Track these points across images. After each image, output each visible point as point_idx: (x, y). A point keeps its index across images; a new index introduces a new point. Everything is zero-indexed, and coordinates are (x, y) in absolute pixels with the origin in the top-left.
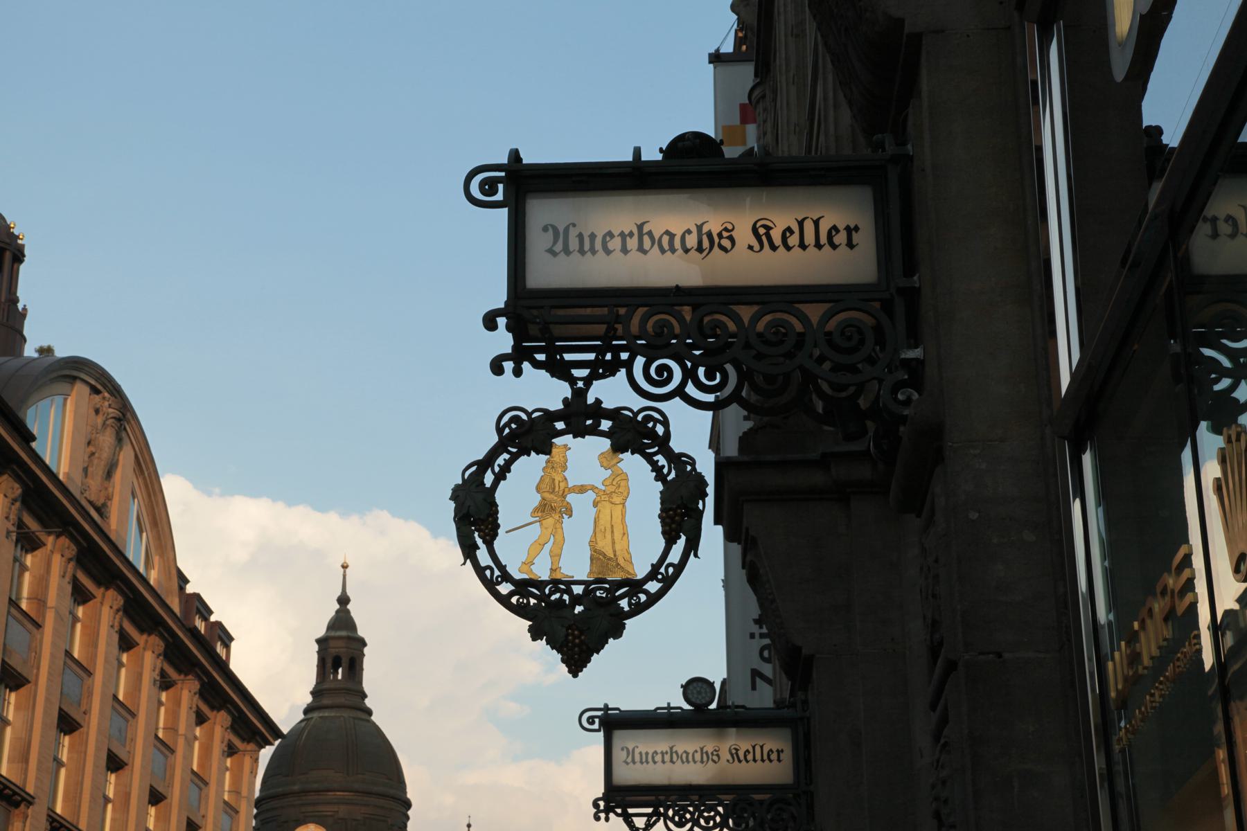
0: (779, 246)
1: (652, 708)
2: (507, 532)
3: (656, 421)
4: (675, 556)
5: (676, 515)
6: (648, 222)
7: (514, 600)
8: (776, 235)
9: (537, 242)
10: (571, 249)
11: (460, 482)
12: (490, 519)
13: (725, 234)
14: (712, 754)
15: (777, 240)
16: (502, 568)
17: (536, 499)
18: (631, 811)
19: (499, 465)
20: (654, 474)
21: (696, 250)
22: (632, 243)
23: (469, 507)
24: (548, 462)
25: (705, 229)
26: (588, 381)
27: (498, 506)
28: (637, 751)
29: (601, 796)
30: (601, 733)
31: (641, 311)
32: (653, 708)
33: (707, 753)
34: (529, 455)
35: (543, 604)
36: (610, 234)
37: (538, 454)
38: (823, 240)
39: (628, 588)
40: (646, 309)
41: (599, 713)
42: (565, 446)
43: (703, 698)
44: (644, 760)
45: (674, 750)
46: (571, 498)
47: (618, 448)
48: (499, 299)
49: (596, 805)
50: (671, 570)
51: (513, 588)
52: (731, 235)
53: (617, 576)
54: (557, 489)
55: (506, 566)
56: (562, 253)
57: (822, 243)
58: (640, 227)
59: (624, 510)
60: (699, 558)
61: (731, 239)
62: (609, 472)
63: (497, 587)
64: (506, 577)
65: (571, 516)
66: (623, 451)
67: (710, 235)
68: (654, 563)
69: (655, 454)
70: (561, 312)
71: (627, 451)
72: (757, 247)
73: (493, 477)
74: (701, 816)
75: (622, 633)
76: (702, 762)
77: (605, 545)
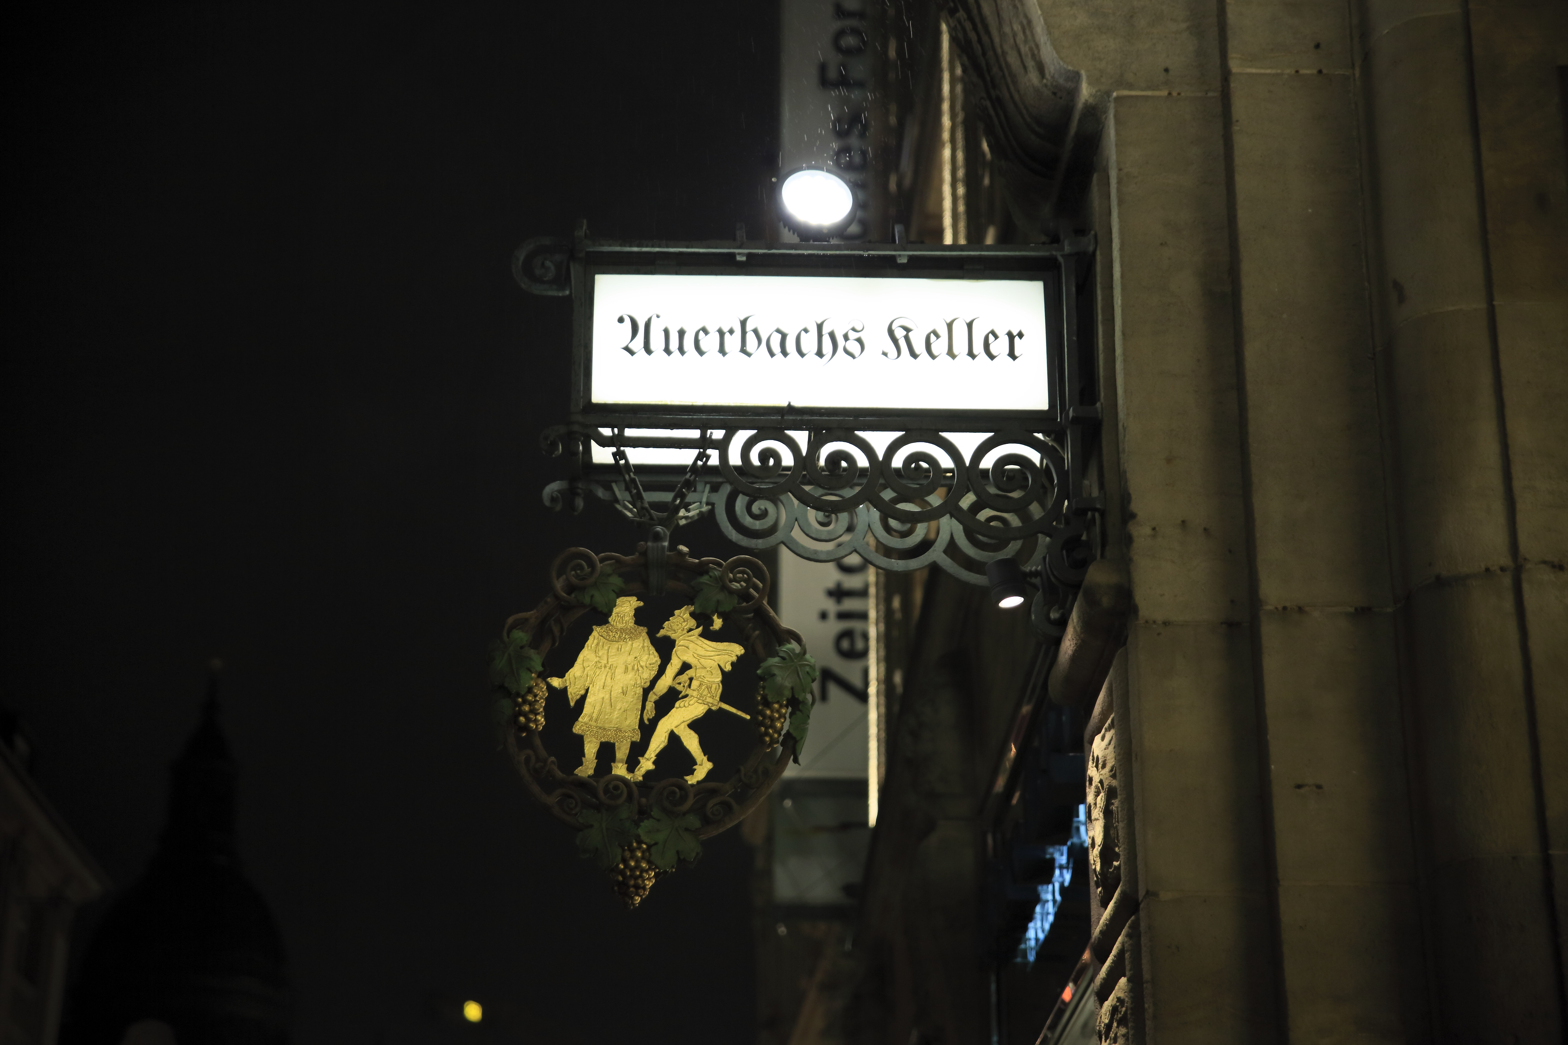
13: (853, 335)
22: (733, 342)
38: (978, 348)
57: (975, 352)
58: (743, 323)
61: (859, 340)
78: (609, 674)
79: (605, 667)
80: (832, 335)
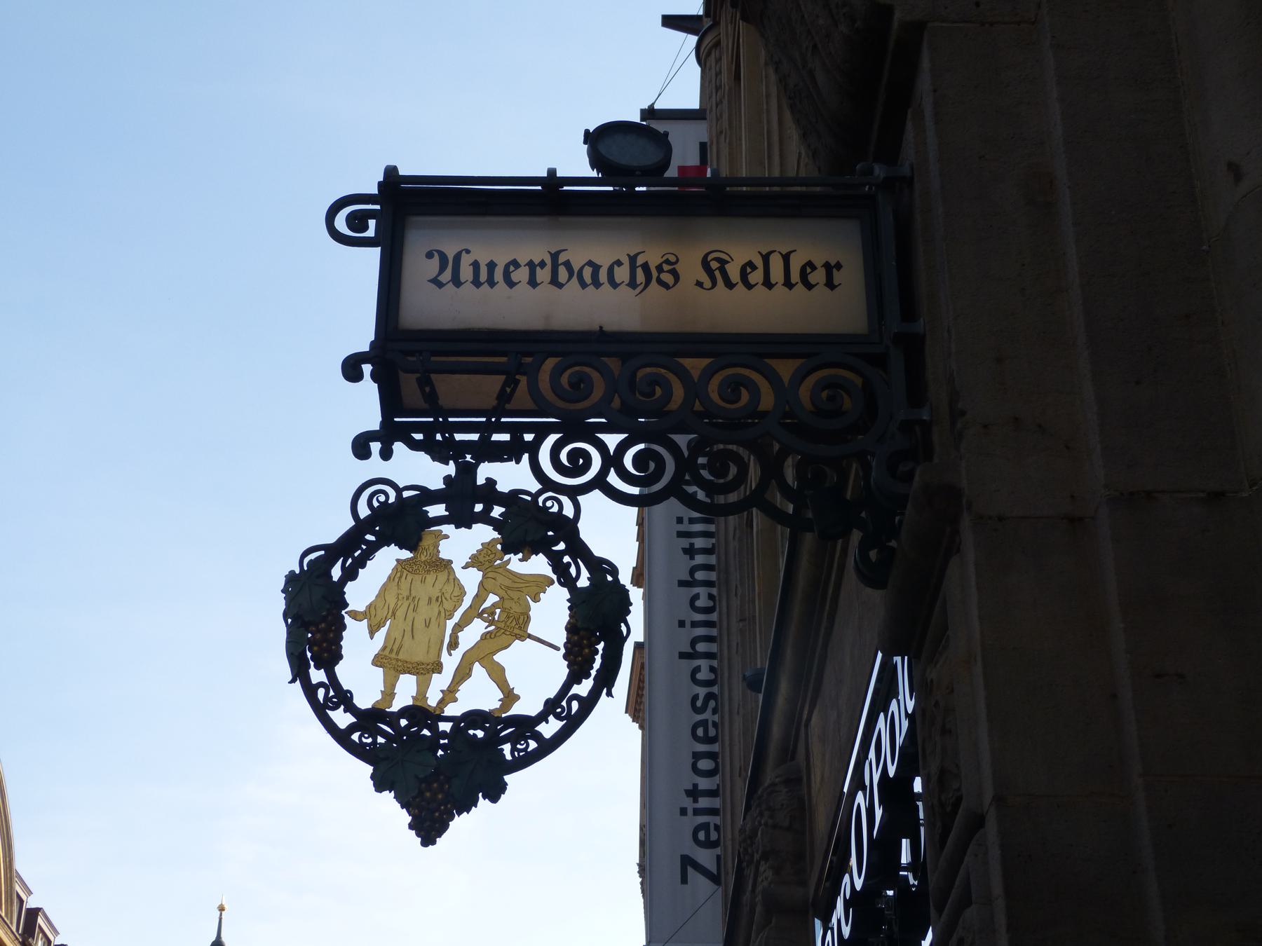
6: (567, 250)
7: (355, 737)
8: (734, 272)
9: (418, 268)
10: (462, 280)
21: (628, 285)
22: (543, 275)
25: (640, 261)
36: (515, 264)
38: (795, 276)
48: (362, 337)
50: (575, 705)
51: (355, 720)
52: (674, 268)
56: (451, 283)
57: (793, 281)
67: (645, 267)
72: (708, 284)
78: (412, 607)
79: (408, 599)
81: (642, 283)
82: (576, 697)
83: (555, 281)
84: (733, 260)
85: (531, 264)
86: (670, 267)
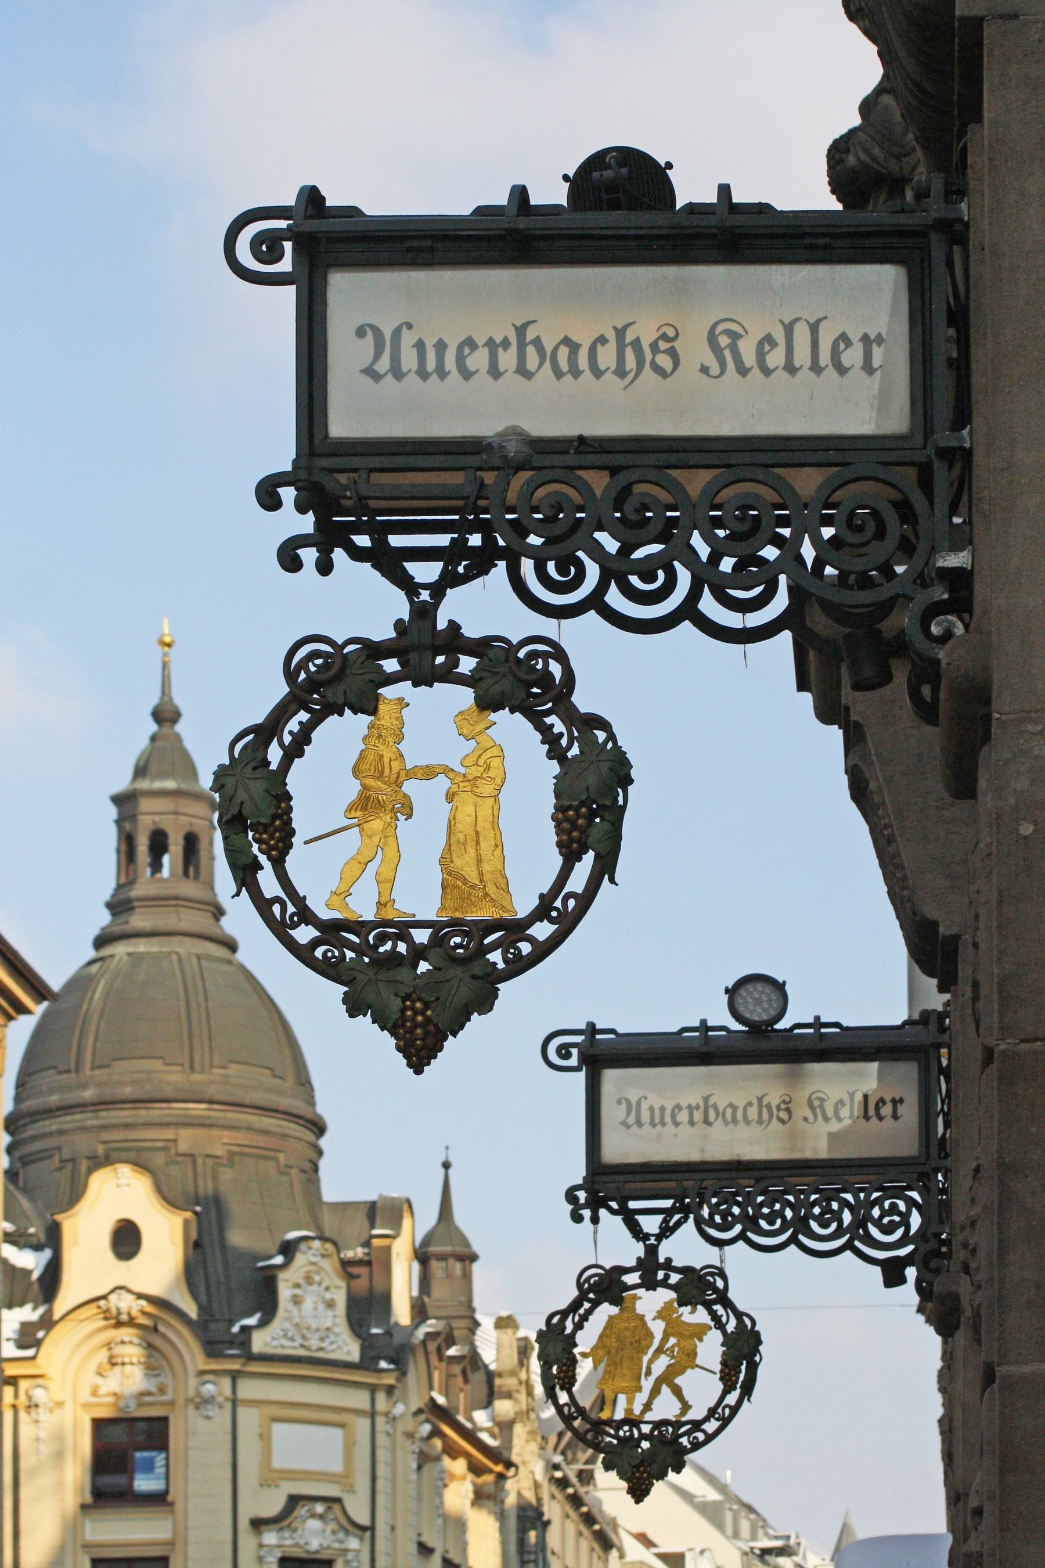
0: (750, 369)
1: (674, 1028)
2: (306, 843)
3: (545, 656)
4: (578, 881)
5: (578, 816)
7: (319, 953)
11: (227, 763)
12: (277, 823)
14: (778, 1108)
15: (749, 358)
16: (300, 902)
17: (353, 789)
18: (633, 1205)
19: (291, 732)
20: (547, 747)
21: (614, 373)
23: (242, 803)
24: (371, 726)
26: (438, 589)
27: (290, 798)
28: (645, 1105)
29: (580, 1182)
30: (581, 1076)
31: (524, 476)
32: (675, 1029)
33: (769, 1106)
34: (341, 714)
35: (367, 960)
37: (355, 713)
38: (825, 358)
39: (503, 933)
40: (532, 473)
41: (579, 1039)
42: (400, 700)
43: (765, 1010)
44: (657, 1120)
45: (711, 1102)
46: (410, 787)
47: (487, 704)
49: (570, 1195)
53: (485, 913)
54: (387, 772)
55: (305, 897)
57: (822, 364)
59: (496, 807)
60: (617, 885)
61: (673, 353)
62: (473, 742)
63: (292, 932)
64: (305, 915)
65: (409, 816)
66: (496, 707)
68: (545, 893)
69: (548, 713)
70: (388, 478)
71: (503, 709)
72: (715, 369)
73: (282, 752)
74: (758, 1215)
75: (493, 1004)
76: (760, 1122)
77: (465, 864)
80: (636, 344)
81: (632, 370)
82: (571, 895)
83: (522, 370)
84: (747, 333)
85: (490, 343)
86: (668, 346)
